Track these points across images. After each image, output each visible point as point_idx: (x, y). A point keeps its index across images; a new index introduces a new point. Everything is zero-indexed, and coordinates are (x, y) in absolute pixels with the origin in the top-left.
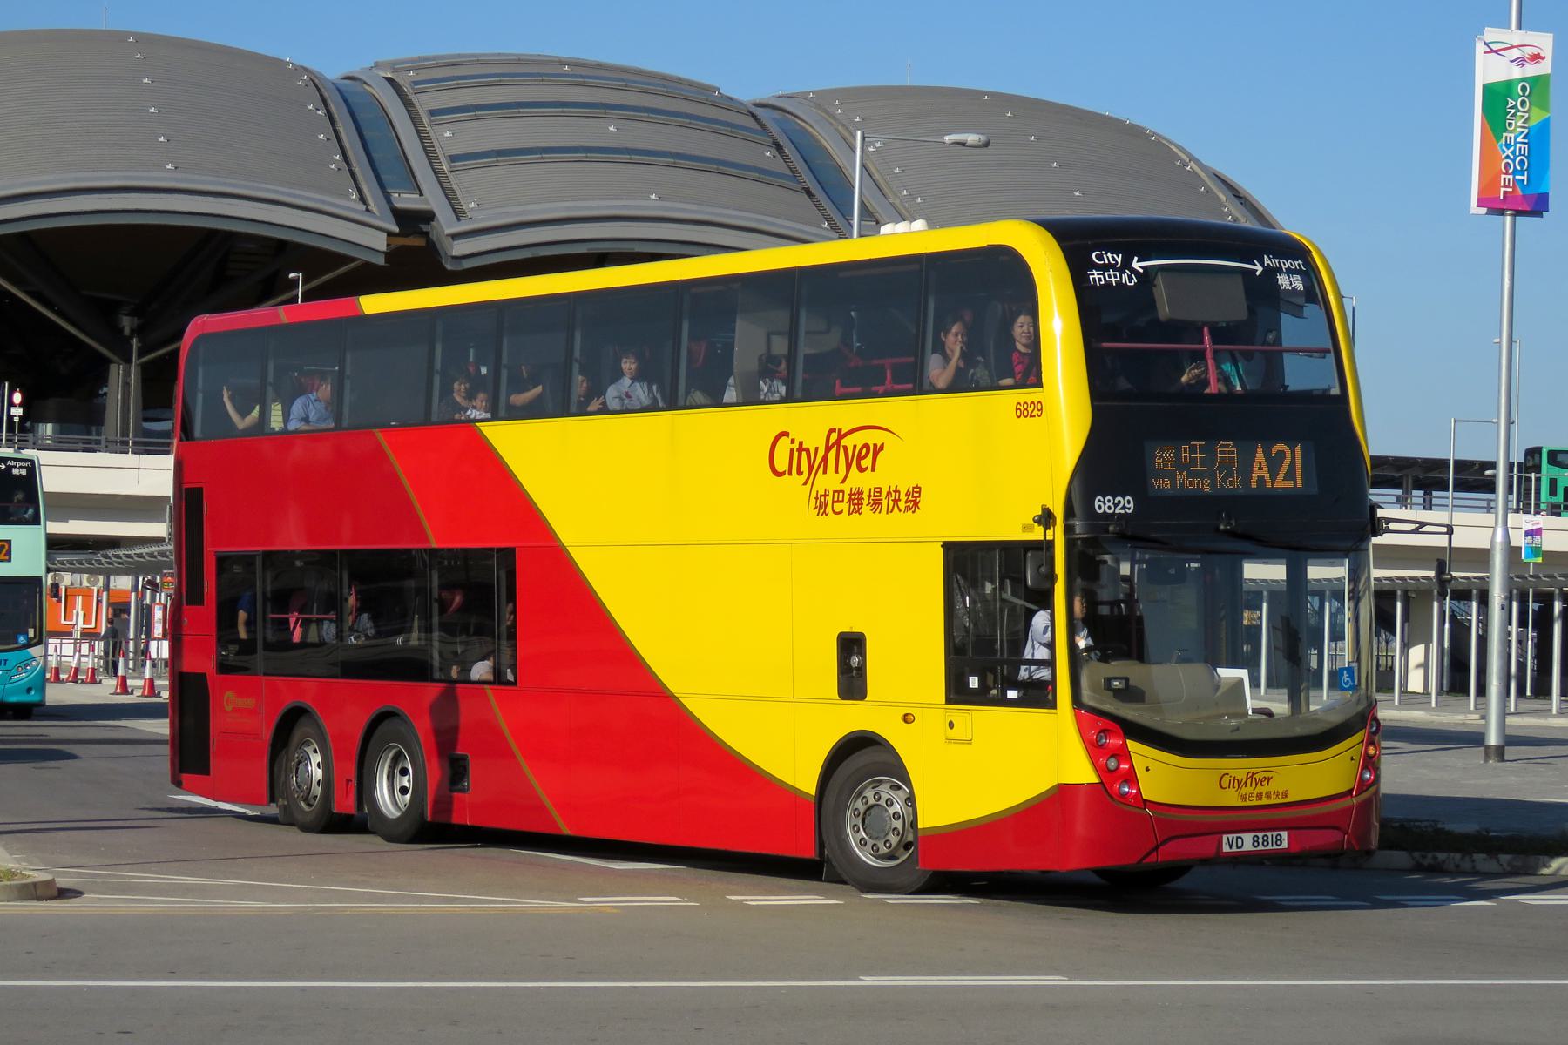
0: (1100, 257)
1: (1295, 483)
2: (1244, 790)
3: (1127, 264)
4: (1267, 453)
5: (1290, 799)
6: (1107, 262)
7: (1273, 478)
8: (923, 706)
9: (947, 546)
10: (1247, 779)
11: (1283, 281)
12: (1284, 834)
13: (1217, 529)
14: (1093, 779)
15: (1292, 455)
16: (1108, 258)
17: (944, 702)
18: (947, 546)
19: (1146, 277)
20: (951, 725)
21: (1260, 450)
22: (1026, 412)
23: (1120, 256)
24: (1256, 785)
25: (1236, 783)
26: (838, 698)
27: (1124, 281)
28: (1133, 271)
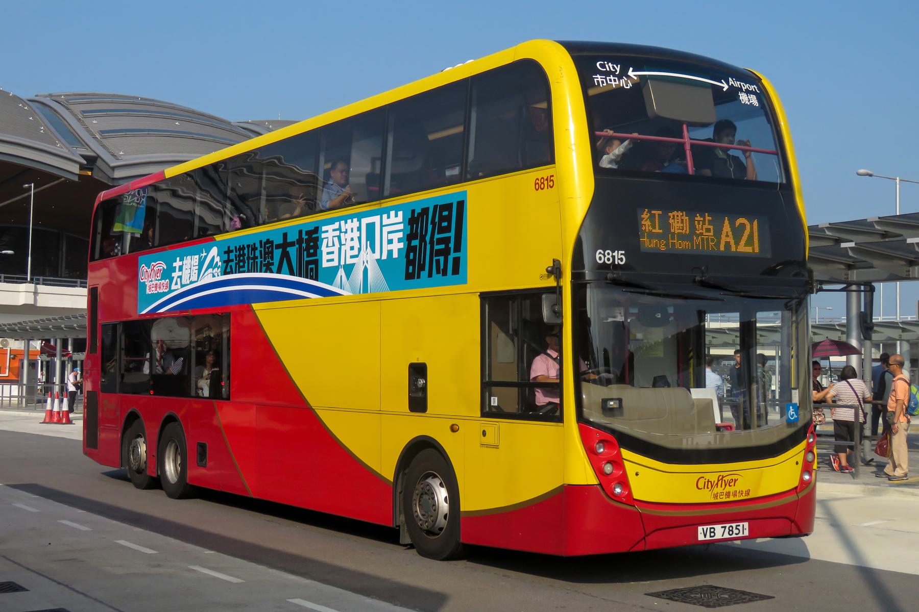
0: (603, 66)
1: (753, 249)
2: (716, 490)
3: (624, 74)
4: (732, 224)
5: (751, 496)
6: (608, 70)
7: (737, 243)
8: (465, 418)
9: (484, 296)
10: (718, 481)
11: (743, 97)
12: (746, 524)
13: (695, 279)
14: (596, 483)
15: (751, 227)
16: (609, 66)
17: (480, 416)
18: (484, 296)
19: (640, 86)
20: (484, 434)
21: (727, 222)
22: (542, 185)
23: (619, 66)
24: (726, 485)
25: (709, 484)
26: (408, 411)
27: (621, 85)
28: (628, 77)
